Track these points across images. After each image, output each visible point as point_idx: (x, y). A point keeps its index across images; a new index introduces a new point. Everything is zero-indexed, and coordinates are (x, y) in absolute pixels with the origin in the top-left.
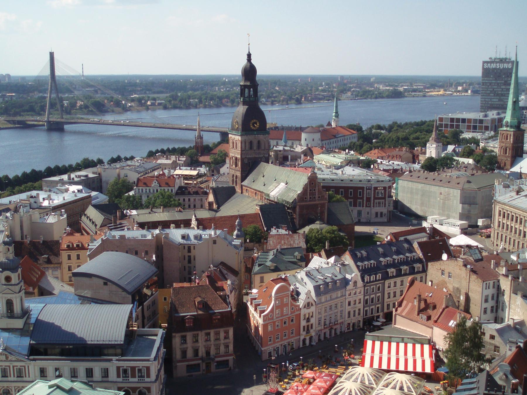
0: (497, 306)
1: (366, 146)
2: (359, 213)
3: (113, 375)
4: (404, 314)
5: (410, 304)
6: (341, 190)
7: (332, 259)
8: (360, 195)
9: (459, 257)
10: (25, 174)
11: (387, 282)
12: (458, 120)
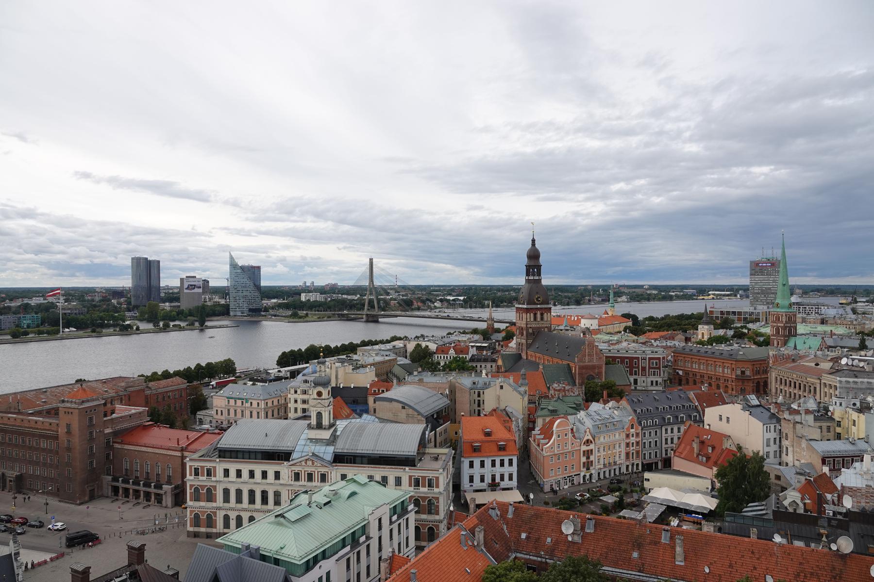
2: (636, 381)
3: (405, 481)
10: (343, 345)
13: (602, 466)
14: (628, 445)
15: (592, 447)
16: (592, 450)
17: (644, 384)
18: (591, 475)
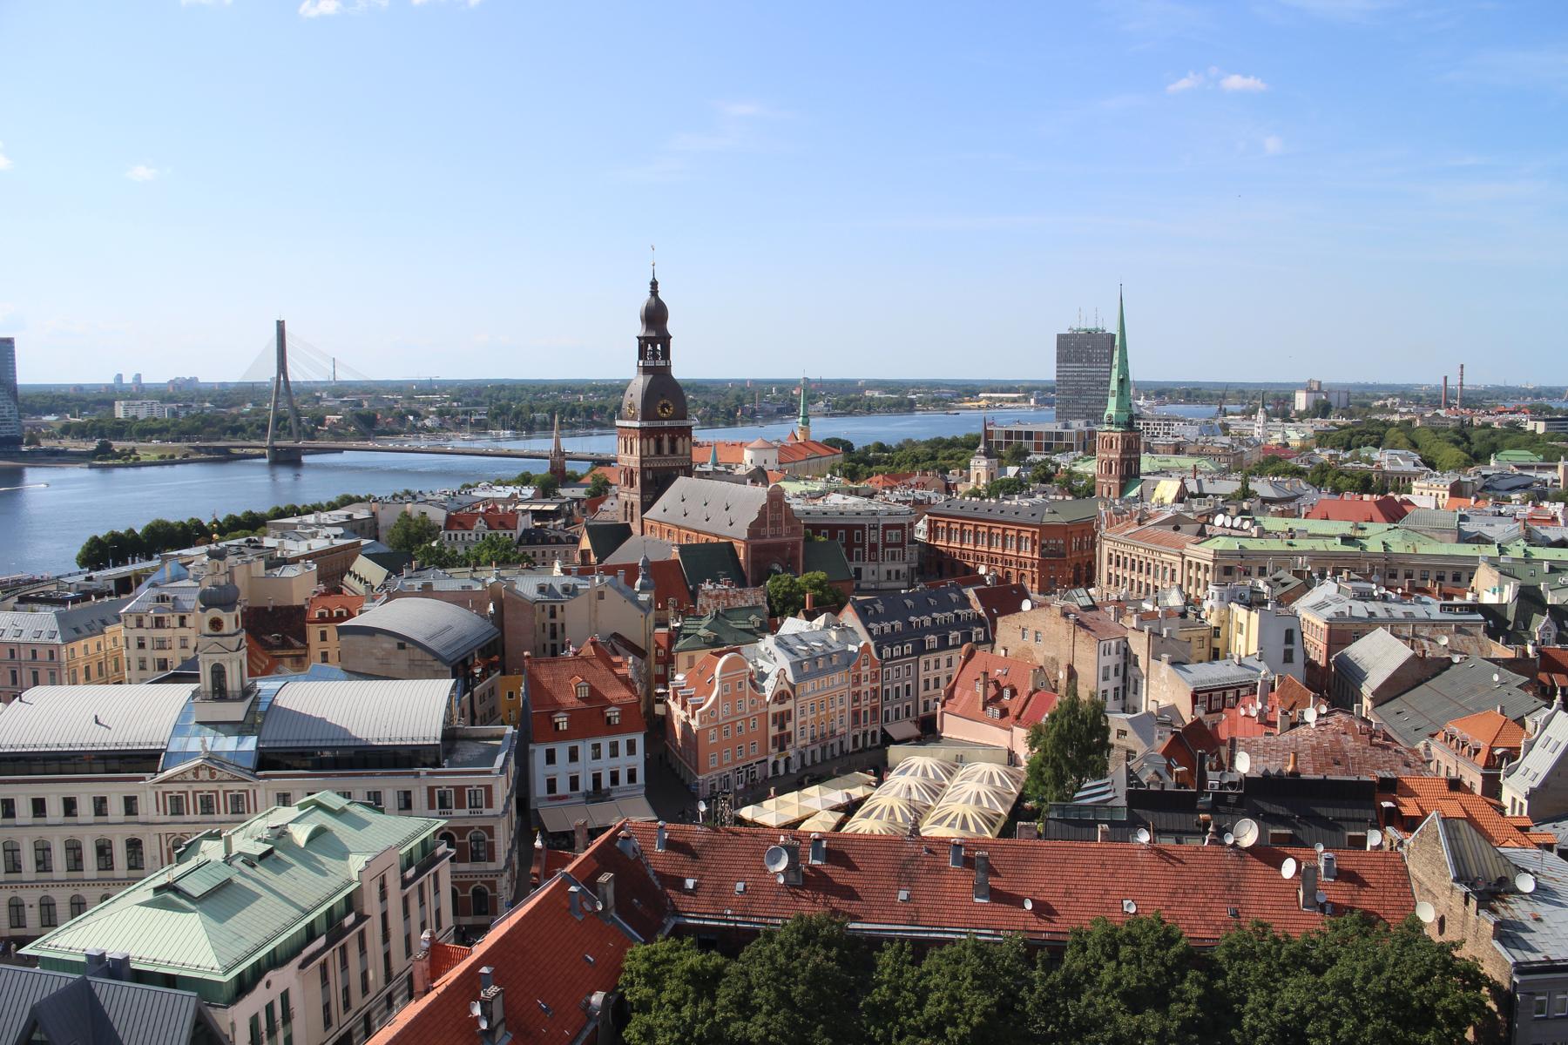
2: (858, 571)
3: (420, 798)
4: (957, 711)
7: (820, 621)
11: (922, 660)
14: (856, 697)
15: (789, 705)
17: (874, 578)
18: (788, 759)
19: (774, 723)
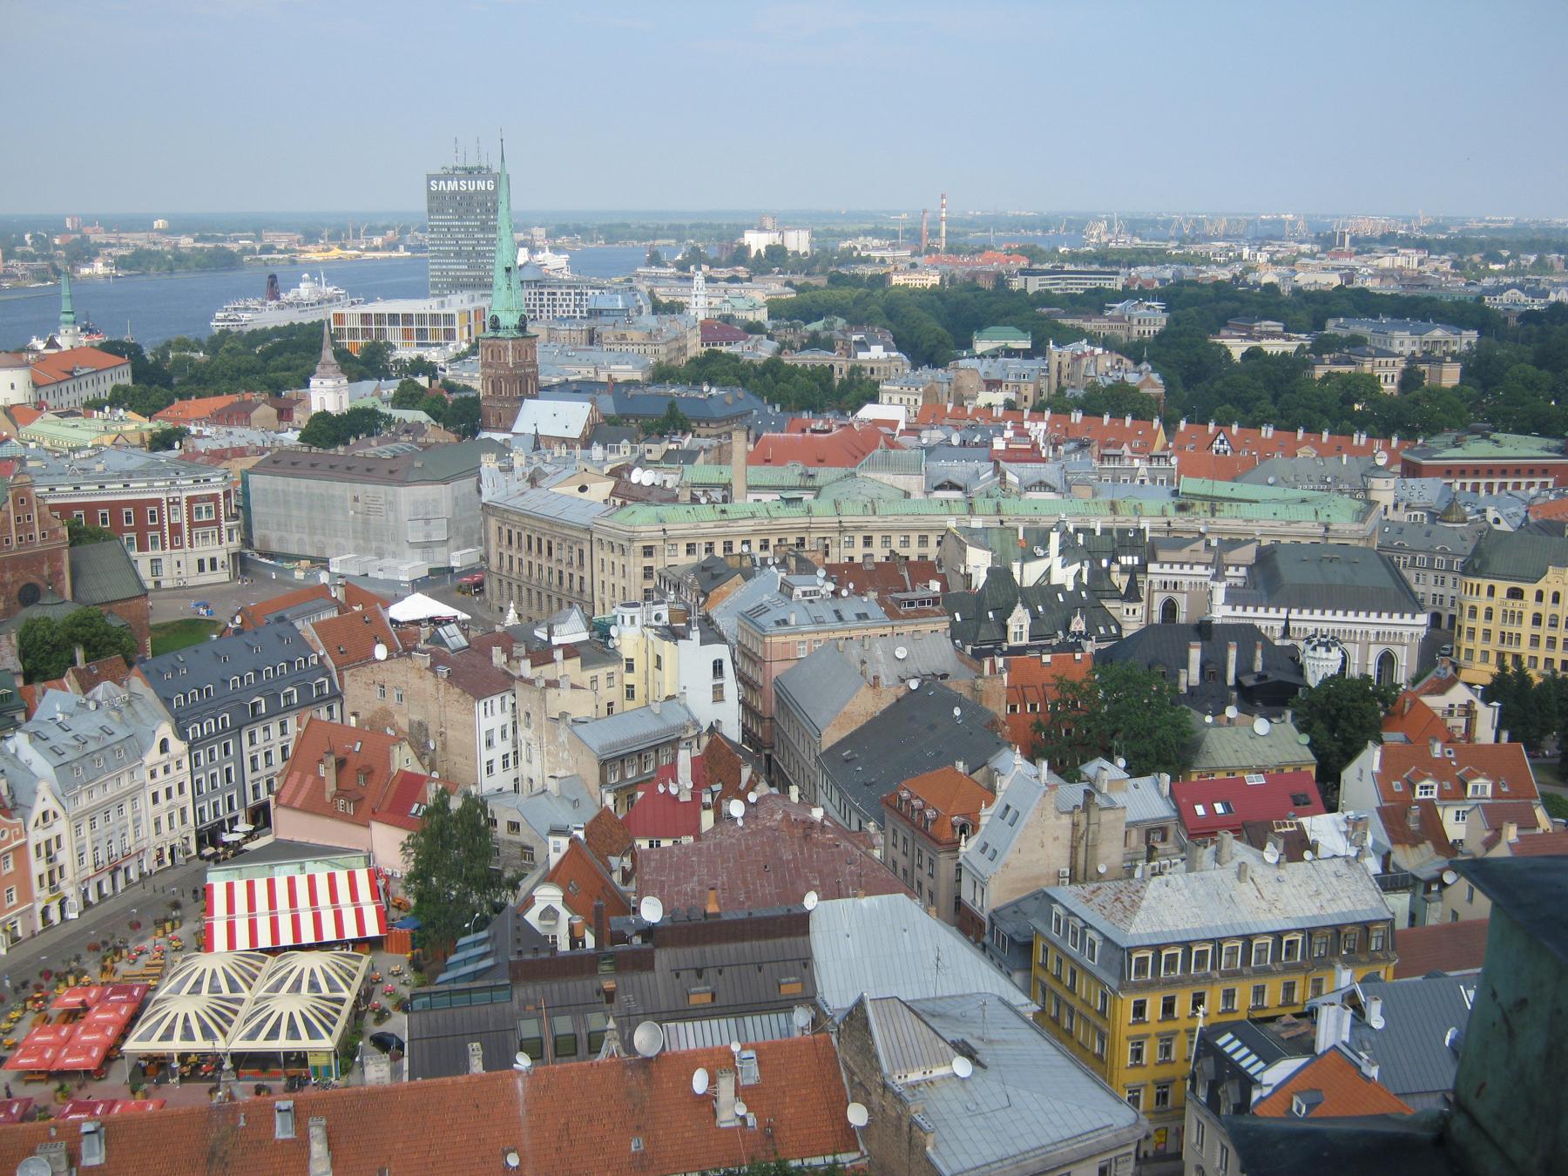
0: (516, 753)
1: (158, 392)
2: (155, 562)
5: (310, 779)
6: (101, 511)
8: (153, 519)
9: (415, 649)
12: (380, 318)
13: (91, 872)
16: (58, 838)
19: (38, 855)
